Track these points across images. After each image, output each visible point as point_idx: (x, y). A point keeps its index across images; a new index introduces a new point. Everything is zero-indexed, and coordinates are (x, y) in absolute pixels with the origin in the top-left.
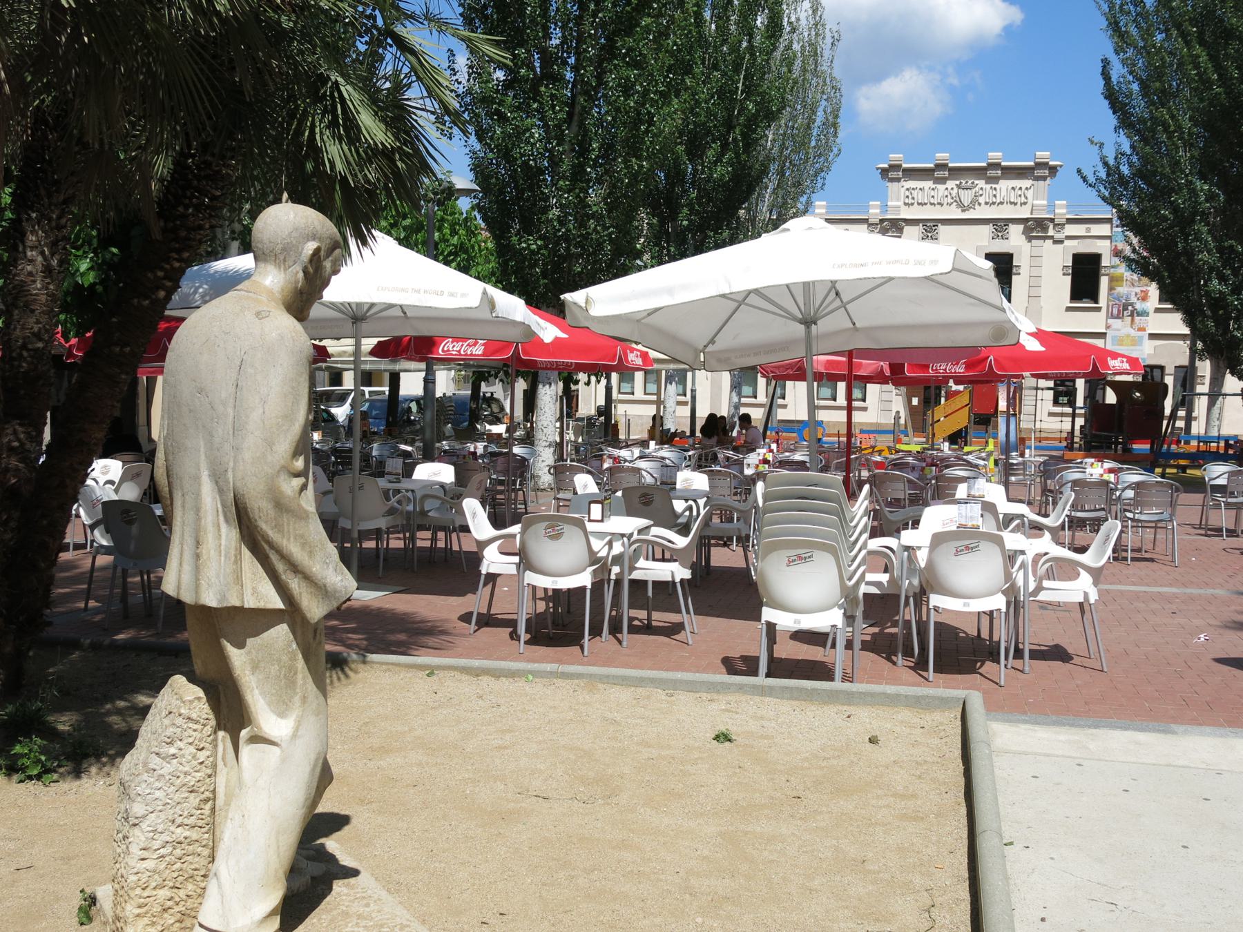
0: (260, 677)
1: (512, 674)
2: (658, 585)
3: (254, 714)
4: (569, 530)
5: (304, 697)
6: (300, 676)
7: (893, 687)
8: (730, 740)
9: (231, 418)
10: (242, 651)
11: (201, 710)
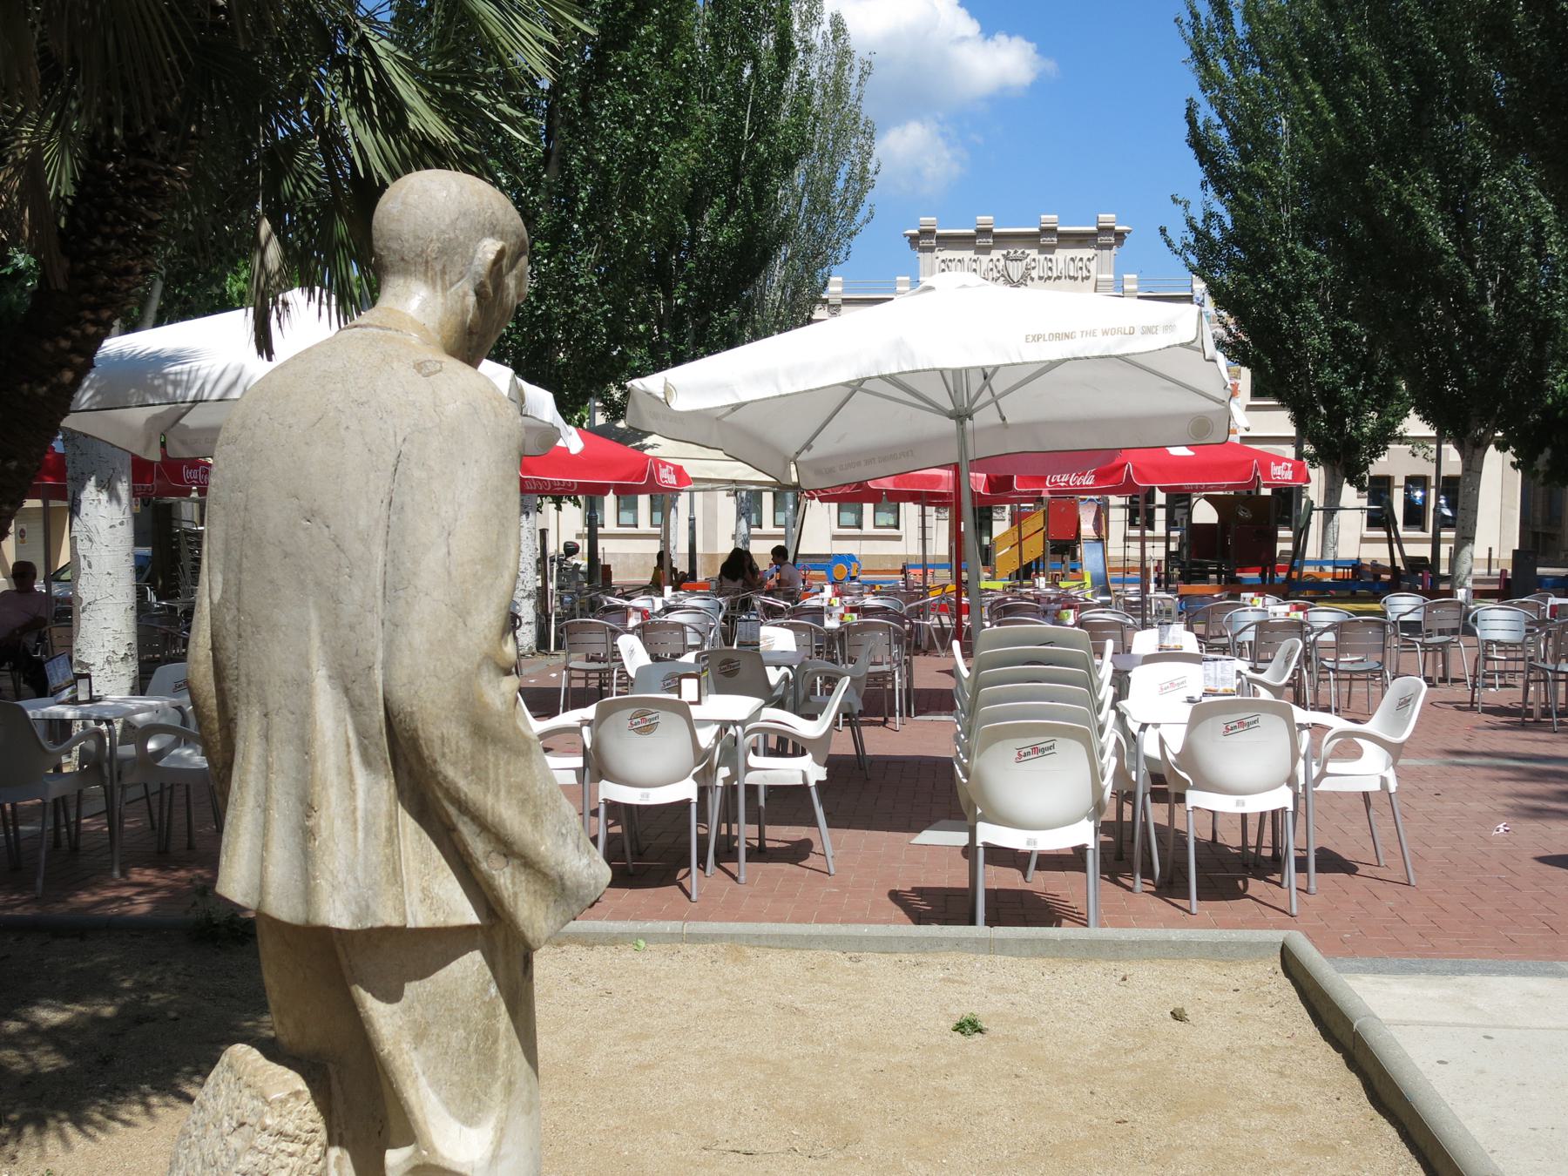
0: (431, 1053)
1: (614, 940)
2: (773, 790)
3: (421, 1124)
4: (666, 719)
5: (510, 1083)
6: (502, 1045)
7: (1178, 931)
8: (980, 1031)
9: (380, 564)
10: (395, 1006)
11: (302, 1113)
